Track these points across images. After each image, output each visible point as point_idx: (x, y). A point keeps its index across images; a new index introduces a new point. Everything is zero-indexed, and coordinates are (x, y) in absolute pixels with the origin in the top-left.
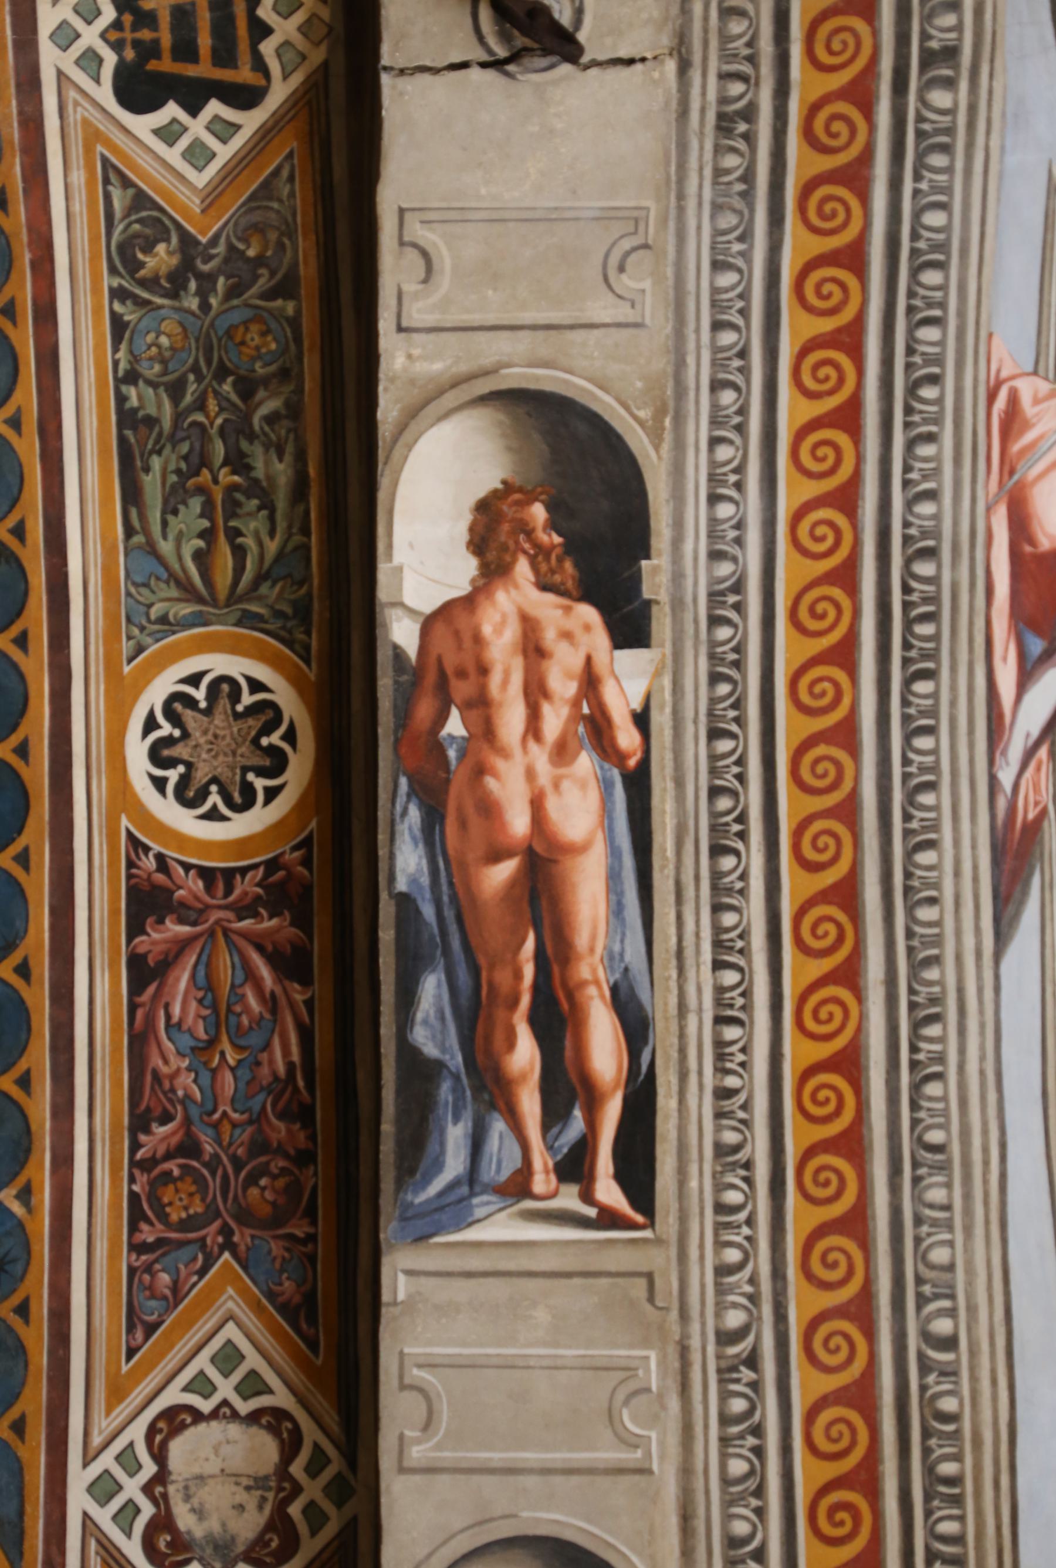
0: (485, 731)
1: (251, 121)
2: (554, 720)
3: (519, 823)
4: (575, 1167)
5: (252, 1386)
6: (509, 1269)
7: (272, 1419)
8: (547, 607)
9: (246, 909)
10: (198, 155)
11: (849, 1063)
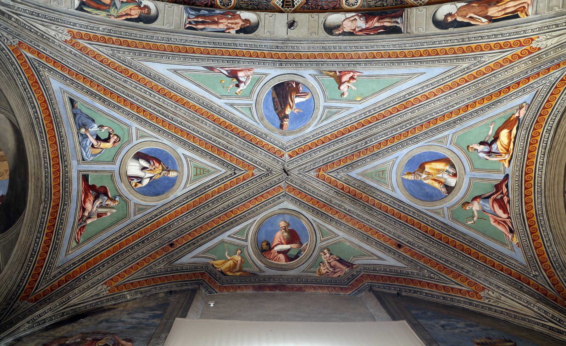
0: (229, 19)
1: (280, 7)
2: (230, 25)
3: (221, 21)
4: (190, 23)
6: (182, 16)
8: (240, 25)
10: (278, 3)
11: (194, 52)
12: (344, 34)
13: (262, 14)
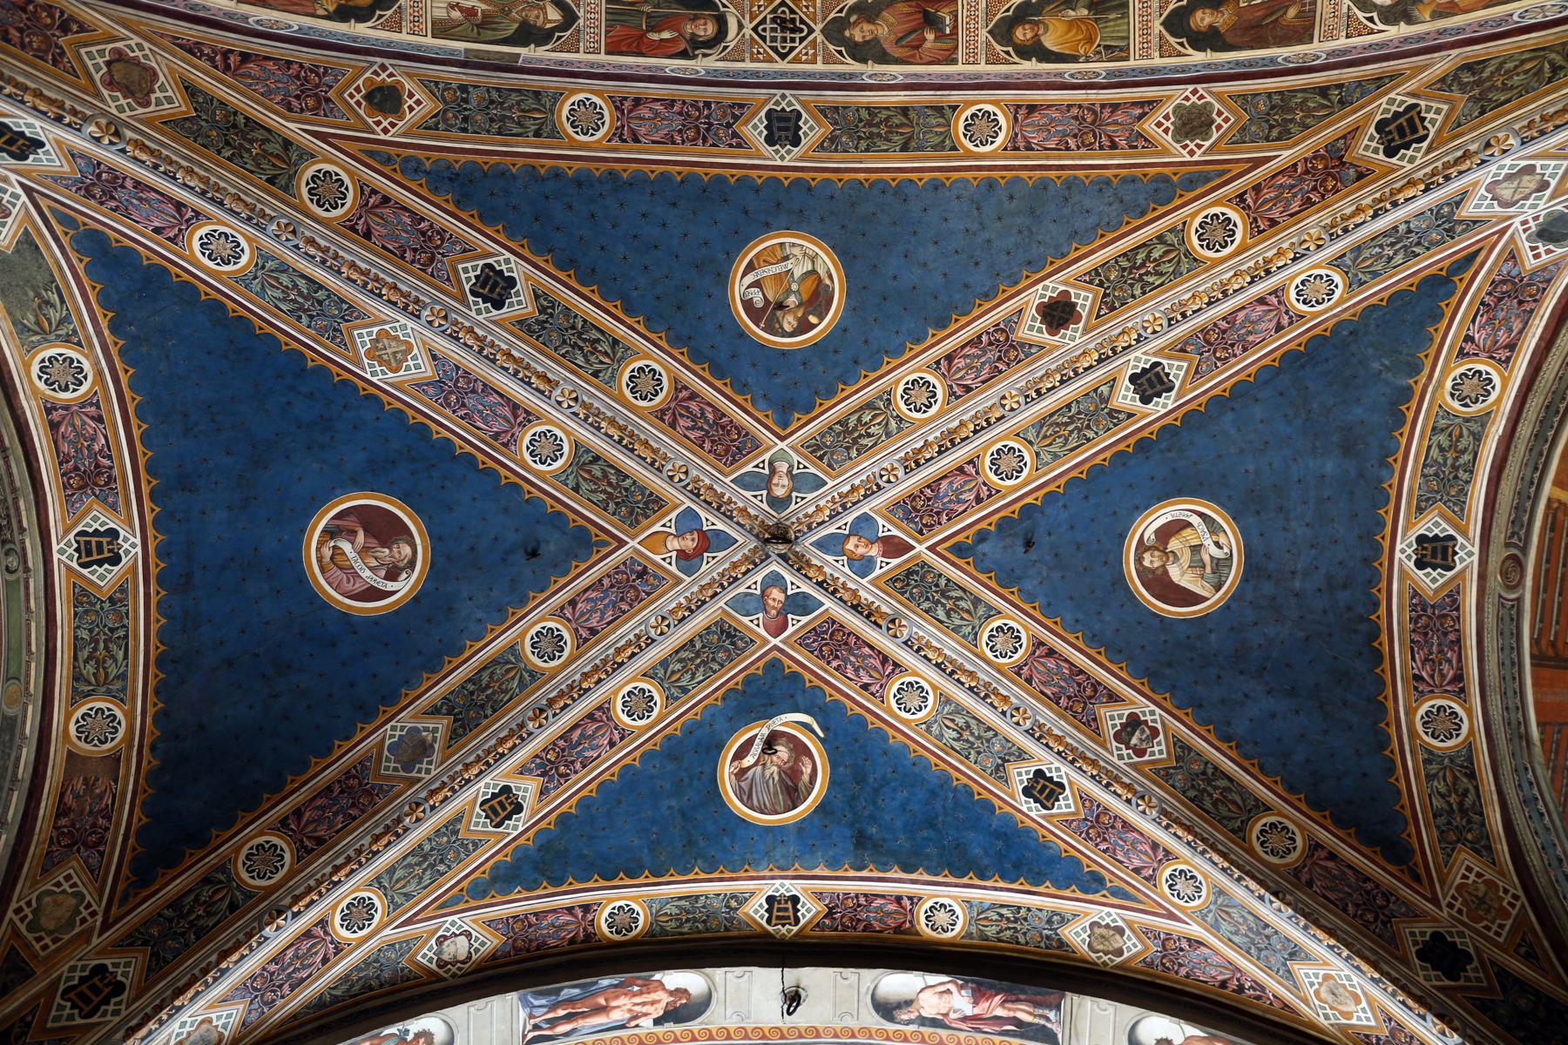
0: (635, 995)
2: (637, 1008)
3: (614, 1004)
4: (536, 1027)
5: (477, 950)
7: (469, 957)
8: (663, 1004)
9: (585, 930)
12: (923, 1021)
13: (718, 973)
